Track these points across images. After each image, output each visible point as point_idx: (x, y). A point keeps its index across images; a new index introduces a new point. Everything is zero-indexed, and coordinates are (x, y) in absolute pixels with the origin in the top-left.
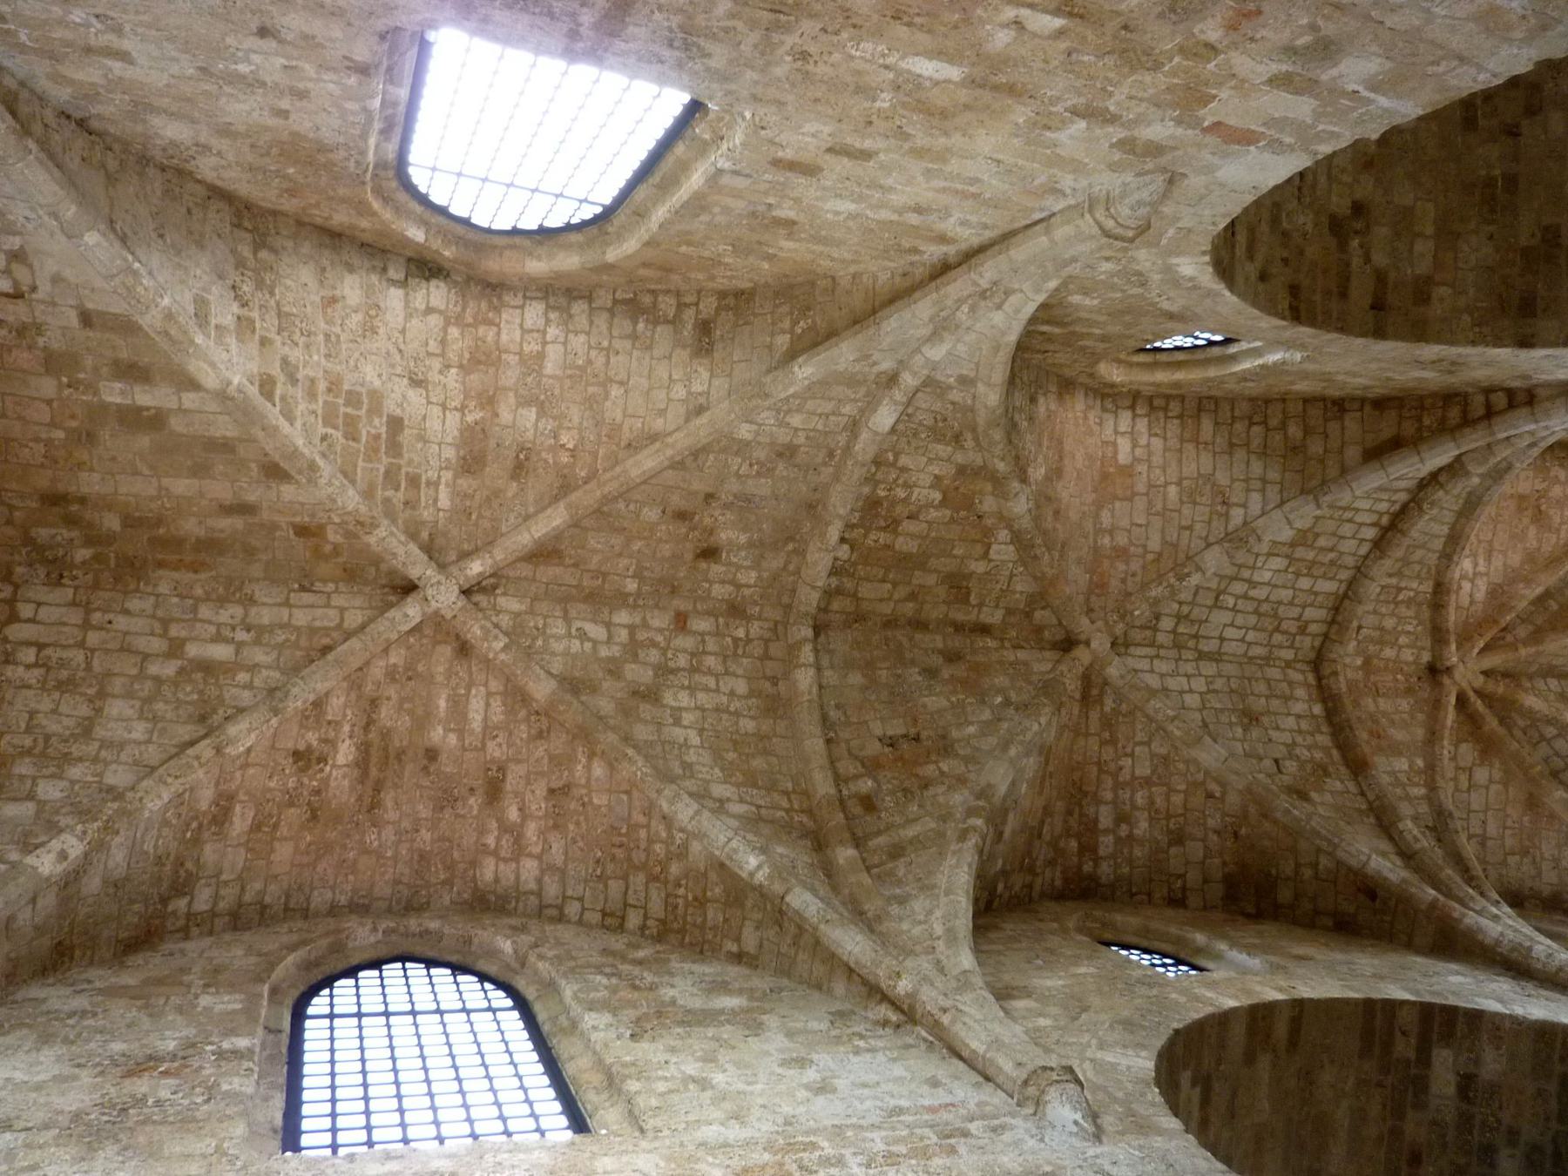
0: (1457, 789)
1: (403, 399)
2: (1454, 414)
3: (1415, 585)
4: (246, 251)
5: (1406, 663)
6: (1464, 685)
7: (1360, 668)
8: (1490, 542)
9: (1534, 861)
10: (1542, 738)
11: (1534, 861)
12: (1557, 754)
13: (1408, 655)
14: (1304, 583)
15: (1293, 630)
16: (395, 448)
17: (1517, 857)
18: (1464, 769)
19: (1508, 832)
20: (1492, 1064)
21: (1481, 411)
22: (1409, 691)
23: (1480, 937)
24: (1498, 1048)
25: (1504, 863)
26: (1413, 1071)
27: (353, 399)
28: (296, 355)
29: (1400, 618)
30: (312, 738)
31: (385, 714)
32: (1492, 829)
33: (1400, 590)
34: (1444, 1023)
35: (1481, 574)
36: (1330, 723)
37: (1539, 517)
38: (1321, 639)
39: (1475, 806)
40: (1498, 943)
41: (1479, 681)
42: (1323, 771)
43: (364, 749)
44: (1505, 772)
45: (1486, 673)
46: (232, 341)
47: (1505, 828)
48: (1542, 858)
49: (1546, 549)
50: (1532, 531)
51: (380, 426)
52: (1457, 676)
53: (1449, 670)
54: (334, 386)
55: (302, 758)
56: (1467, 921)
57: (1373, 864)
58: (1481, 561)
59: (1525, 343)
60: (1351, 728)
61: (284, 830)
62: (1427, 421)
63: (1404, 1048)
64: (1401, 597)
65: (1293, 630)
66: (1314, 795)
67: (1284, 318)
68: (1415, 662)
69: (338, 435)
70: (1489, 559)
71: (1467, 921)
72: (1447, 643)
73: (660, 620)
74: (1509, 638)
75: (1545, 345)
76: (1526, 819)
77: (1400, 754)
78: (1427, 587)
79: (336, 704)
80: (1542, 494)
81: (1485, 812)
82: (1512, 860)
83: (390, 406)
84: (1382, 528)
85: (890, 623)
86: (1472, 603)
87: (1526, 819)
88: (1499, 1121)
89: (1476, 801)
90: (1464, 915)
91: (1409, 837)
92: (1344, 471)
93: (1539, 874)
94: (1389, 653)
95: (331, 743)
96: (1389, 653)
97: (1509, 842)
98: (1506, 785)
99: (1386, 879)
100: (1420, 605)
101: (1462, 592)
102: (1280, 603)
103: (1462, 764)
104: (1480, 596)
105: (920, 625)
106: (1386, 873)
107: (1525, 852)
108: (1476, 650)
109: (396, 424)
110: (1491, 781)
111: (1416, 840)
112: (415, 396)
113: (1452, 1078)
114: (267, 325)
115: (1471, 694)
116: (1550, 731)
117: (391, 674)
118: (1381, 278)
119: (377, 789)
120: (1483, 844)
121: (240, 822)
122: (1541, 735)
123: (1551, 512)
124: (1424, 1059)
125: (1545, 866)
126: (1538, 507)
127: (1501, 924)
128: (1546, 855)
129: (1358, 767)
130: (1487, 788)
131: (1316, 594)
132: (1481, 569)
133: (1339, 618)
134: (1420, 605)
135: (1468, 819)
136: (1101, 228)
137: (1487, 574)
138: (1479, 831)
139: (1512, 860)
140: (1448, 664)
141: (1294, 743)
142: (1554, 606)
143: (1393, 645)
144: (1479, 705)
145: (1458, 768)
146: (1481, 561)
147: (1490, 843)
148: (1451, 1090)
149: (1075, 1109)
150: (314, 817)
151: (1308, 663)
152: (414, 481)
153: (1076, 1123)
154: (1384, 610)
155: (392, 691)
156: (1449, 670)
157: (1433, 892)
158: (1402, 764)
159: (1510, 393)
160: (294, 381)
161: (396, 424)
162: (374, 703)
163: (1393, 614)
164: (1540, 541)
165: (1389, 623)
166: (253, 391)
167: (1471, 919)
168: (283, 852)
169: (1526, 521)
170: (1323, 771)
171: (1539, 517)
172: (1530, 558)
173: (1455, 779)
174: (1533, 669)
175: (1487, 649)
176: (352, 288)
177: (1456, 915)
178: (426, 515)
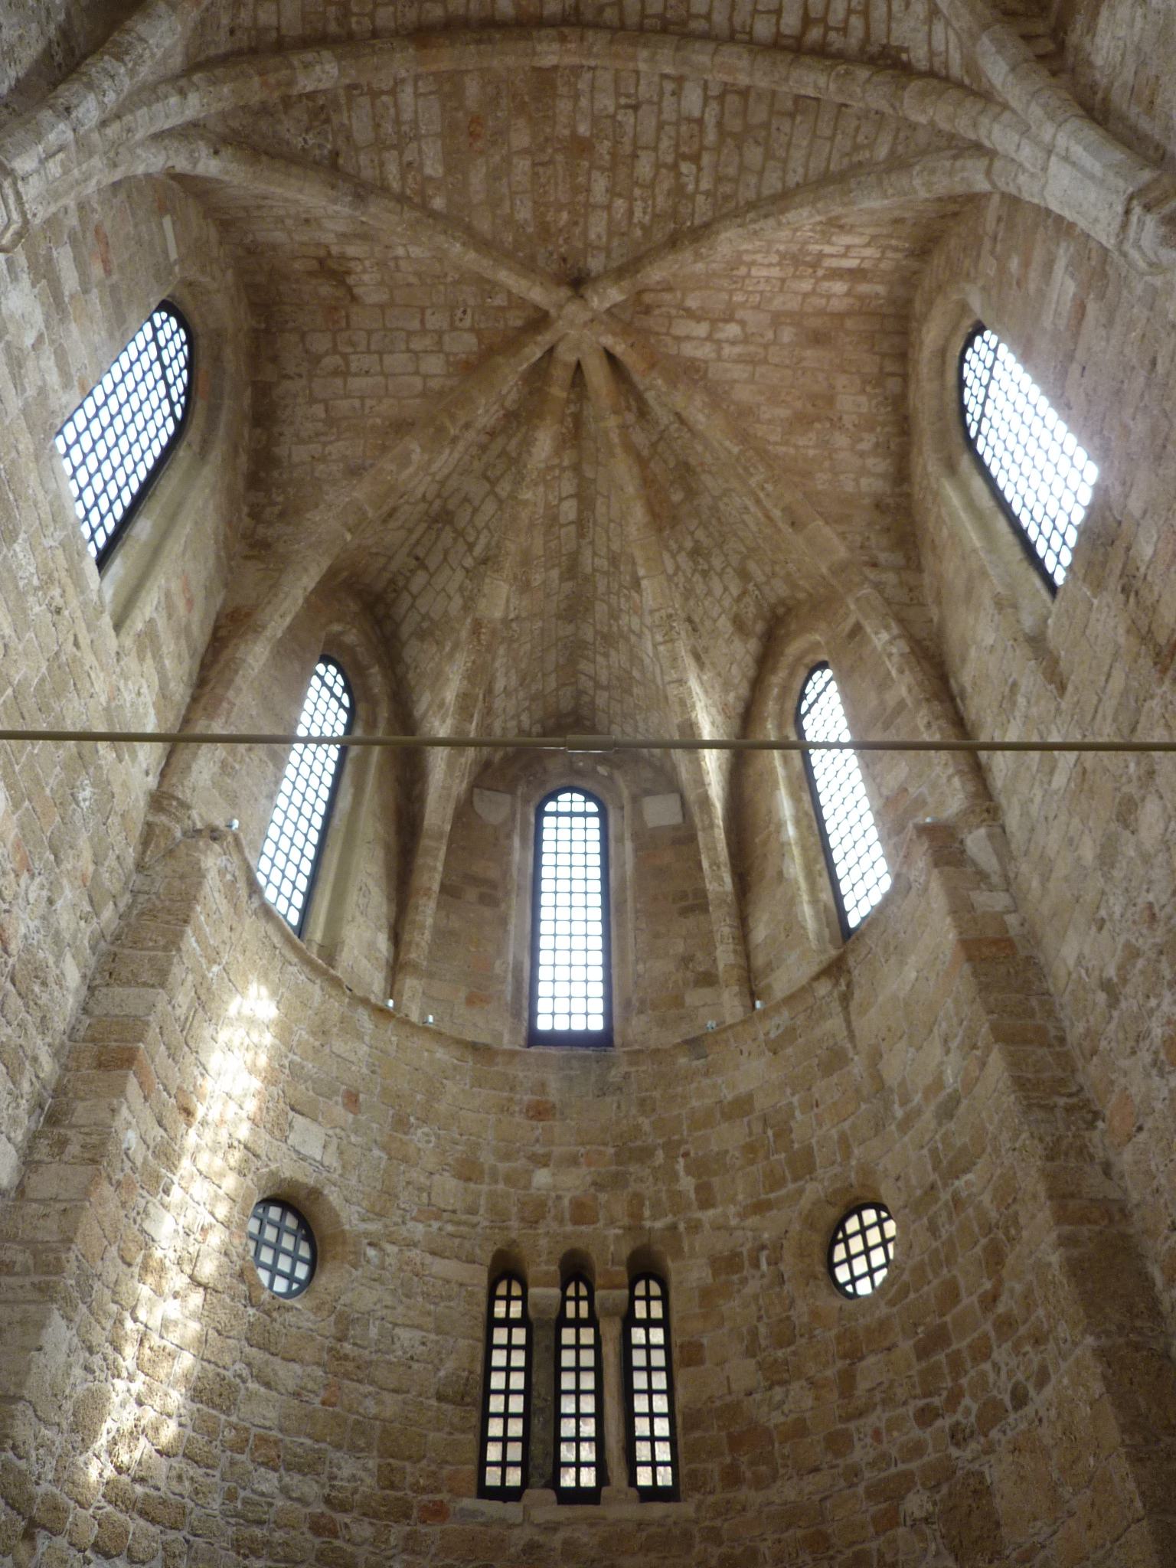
0: (410, 334)
3: (705, 185)
5: (585, 233)
7: (574, 134)
8: (765, 361)
9: (317, 435)
10: (493, 483)
11: (317, 435)
12: (475, 510)
13: (597, 227)
17: (323, 415)
18: (440, 342)
19: (357, 403)
22: (545, 231)
25: (312, 400)
29: (652, 185)
32: (357, 383)
33: (695, 159)
35: (719, 351)
37: (802, 421)
38: (616, 22)
39: (388, 359)
41: (567, 356)
44: (441, 394)
47: (362, 398)
48: (325, 444)
49: (761, 430)
50: (783, 413)
52: (572, 308)
58: (738, 349)
60: (479, 42)
64: (685, 167)
68: (588, 245)
70: (739, 360)
76: (378, 421)
77: (449, 170)
78: (703, 208)
80: (836, 424)
81: (382, 373)
82: (319, 410)
84: (799, 38)
86: (678, 339)
87: (378, 421)
89: (397, 361)
93: (301, 441)
94: (600, 184)
96: (600, 184)
97: (343, 405)
98: (424, 394)
100: (674, 214)
101: (692, 324)
103: (446, 338)
104: (689, 350)
107: (330, 422)
110: (426, 377)
116: (504, 488)
120: (336, 373)
122: (498, 479)
123: (812, 435)
125: (315, 448)
126: (818, 419)
128: (329, 448)
129: (422, 35)
130: (417, 373)
132: (727, 350)
134: (674, 214)
135: (369, 352)
137: (719, 358)
138: (354, 367)
139: (319, 410)
142: (677, 497)
143: (611, 192)
144: (534, 352)
145: (440, 333)
146: (738, 349)
147: (339, 381)
151: (577, 8)
154: (665, 143)
158: (433, 168)
163: (658, 166)
164: (770, 422)
165: (644, 168)
169: (799, 404)
171: (802, 421)
172: (746, 412)
173: (424, 331)
174: (589, 473)
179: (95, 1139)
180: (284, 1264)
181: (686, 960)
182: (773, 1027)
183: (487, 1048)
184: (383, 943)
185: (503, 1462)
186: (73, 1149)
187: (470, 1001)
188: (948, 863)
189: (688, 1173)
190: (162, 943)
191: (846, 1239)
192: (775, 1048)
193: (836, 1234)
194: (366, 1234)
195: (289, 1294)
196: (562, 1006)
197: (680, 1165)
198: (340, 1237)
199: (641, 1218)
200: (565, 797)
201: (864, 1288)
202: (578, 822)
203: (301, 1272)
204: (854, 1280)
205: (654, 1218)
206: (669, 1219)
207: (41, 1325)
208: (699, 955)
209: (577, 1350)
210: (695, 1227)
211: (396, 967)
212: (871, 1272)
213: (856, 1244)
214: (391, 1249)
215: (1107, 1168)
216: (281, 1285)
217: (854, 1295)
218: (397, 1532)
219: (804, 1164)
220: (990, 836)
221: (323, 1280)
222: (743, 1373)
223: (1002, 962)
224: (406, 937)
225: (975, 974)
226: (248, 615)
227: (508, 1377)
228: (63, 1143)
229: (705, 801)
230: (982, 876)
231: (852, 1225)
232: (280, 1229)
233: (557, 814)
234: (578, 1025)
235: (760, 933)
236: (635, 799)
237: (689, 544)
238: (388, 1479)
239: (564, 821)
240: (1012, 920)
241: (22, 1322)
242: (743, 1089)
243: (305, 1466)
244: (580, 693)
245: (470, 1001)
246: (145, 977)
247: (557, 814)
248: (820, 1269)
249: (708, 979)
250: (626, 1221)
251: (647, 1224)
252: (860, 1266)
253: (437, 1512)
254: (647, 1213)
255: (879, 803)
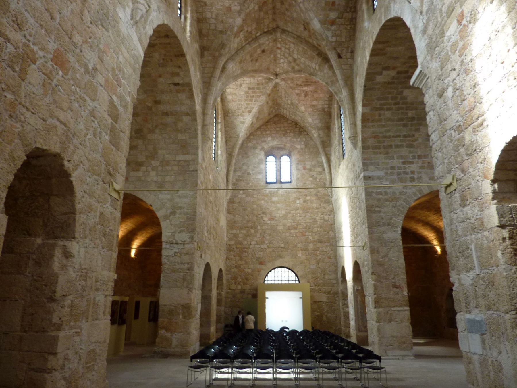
1: (245, 87)
4: (231, 115)
16: (253, 88)
27: (247, 97)
28: (243, 107)
30: (303, 95)
31: (299, 83)
43: (305, 85)
46: (245, 117)
51: (250, 91)
54: (246, 100)
55: (306, 95)
61: (318, 96)
69: (254, 99)
73: (279, 51)
79: (297, 91)
83: (247, 89)
85: (274, 13)
95: (304, 91)
105: (274, 8)
109: (249, 88)
112: (244, 85)
114: (240, 112)
117: (292, 83)
119: (312, 82)
121: (315, 103)
150: (316, 92)
152: (258, 84)
155: (295, 82)
160: (247, 107)
161: (249, 88)
162: (297, 85)
166: (251, 114)
168: (321, 95)
176: (229, 97)
178: (264, 81)
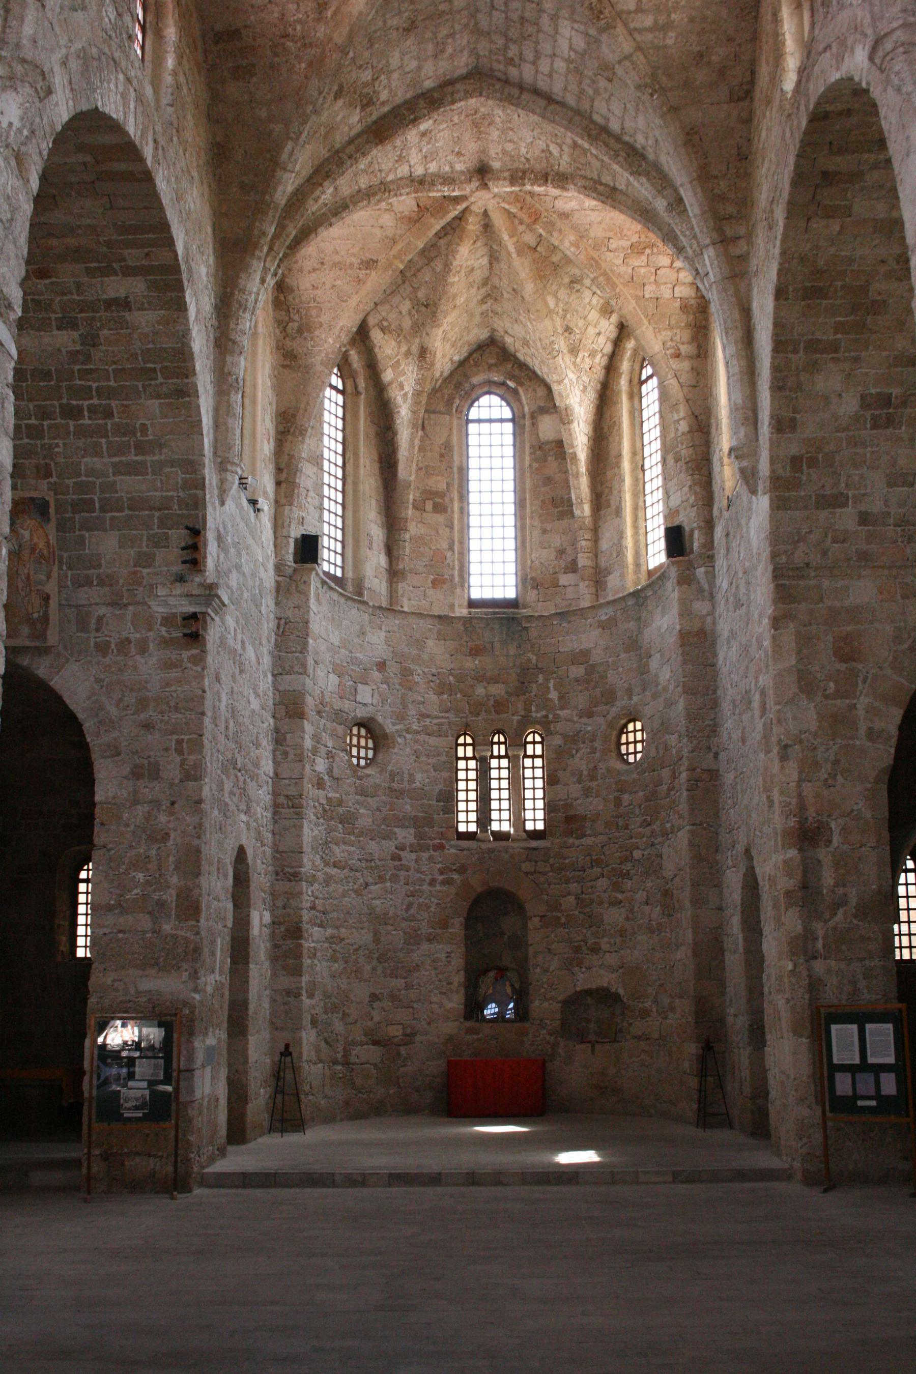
2: (731, 209)
6: (472, 199)
14: (560, 65)
15: (510, 54)
20: (144, 320)
21: (729, 232)
23: (243, 275)
24: (159, 323)
26: (116, 266)
34: (168, 282)
36: (417, 97)
40: (243, 291)
42: (368, 102)
45: (486, 214)
53: (485, 186)
56: (255, 262)
57: (286, 175)
59: (780, 293)
62: (723, 184)
63: (133, 256)
65: (510, 54)
66: (340, 102)
67: (815, 108)
71: (255, 262)
72: (512, 184)
74: (521, 228)
75: (777, 309)
88: (100, 329)
90: (259, 258)
91: (317, 193)
92: (674, 109)
99: (275, 190)
102: (537, 43)
106: (280, 189)
108: (507, 207)
111: (316, 200)
113: (122, 293)
115: (464, 206)
118: (855, 177)
124: (129, 272)
127: (257, 289)
131: (550, 76)
133: (525, 96)
136: (886, 35)
140: (490, 184)
141: (391, 72)
148: (112, 294)
149: (22, 119)
153: (11, 124)
156: (485, 186)
157: (272, 230)
159: (744, 258)
164: (616, 250)
167: (257, 267)
170: (368, 102)
175: (511, 216)
177: (257, 253)
179: (299, 752)
180: (362, 754)
181: (561, 552)
182: (604, 615)
183: (446, 617)
184: (383, 560)
185: (467, 822)
186: (291, 756)
187: (435, 584)
188: (684, 583)
189: (555, 689)
190: (299, 649)
191: (627, 732)
192: (603, 626)
193: (623, 730)
194: (397, 731)
195: (367, 765)
196: (487, 580)
197: (551, 685)
198: (385, 736)
199: (530, 711)
200: (485, 400)
201: (631, 759)
202: (496, 426)
203: (371, 754)
204: (628, 754)
205: (537, 712)
206: (544, 713)
207: (302, 827)
208: (569, 550)
209: (499, 770)
210: (557, 718)
211: (394, 574)
212: (635, 753)
213: (631, 737)
214: (409, 736)
215: (716, 755)
216: (362, 762)
217: (626, 762)
218: (425, 855)
219: (610, 696)
220: (706, 573)
221: (380, 756)
222: (575, 790)
223: (698, 643)
224: (395, 553)
225: (683, 654)
226: (294, 416)
227: (467, 772)
228: (286, 754)
229: (574, 457)
230: (701, 590)
231: (631, 727)
232: (359, 736)
233: (479, 421)
234: (499, 594)
235: (604, 545)
236: (533, 416)
237: (566, 280)
238: (420, 836)
239: (485, 427)
240: (709, 619)
241: (294, 826)
242: (584, 646)
243: (387, 836)
244: (493, 330)
245: (435, 584)
246: (296, 668)
247: (479, 421)
248: (613, 746)
249: (572, 568)
250: (522, 713)
251: (534, 715)
252: (631, 748)
253: (441, 847)
254: (533, 709)
255: (667, 512)
